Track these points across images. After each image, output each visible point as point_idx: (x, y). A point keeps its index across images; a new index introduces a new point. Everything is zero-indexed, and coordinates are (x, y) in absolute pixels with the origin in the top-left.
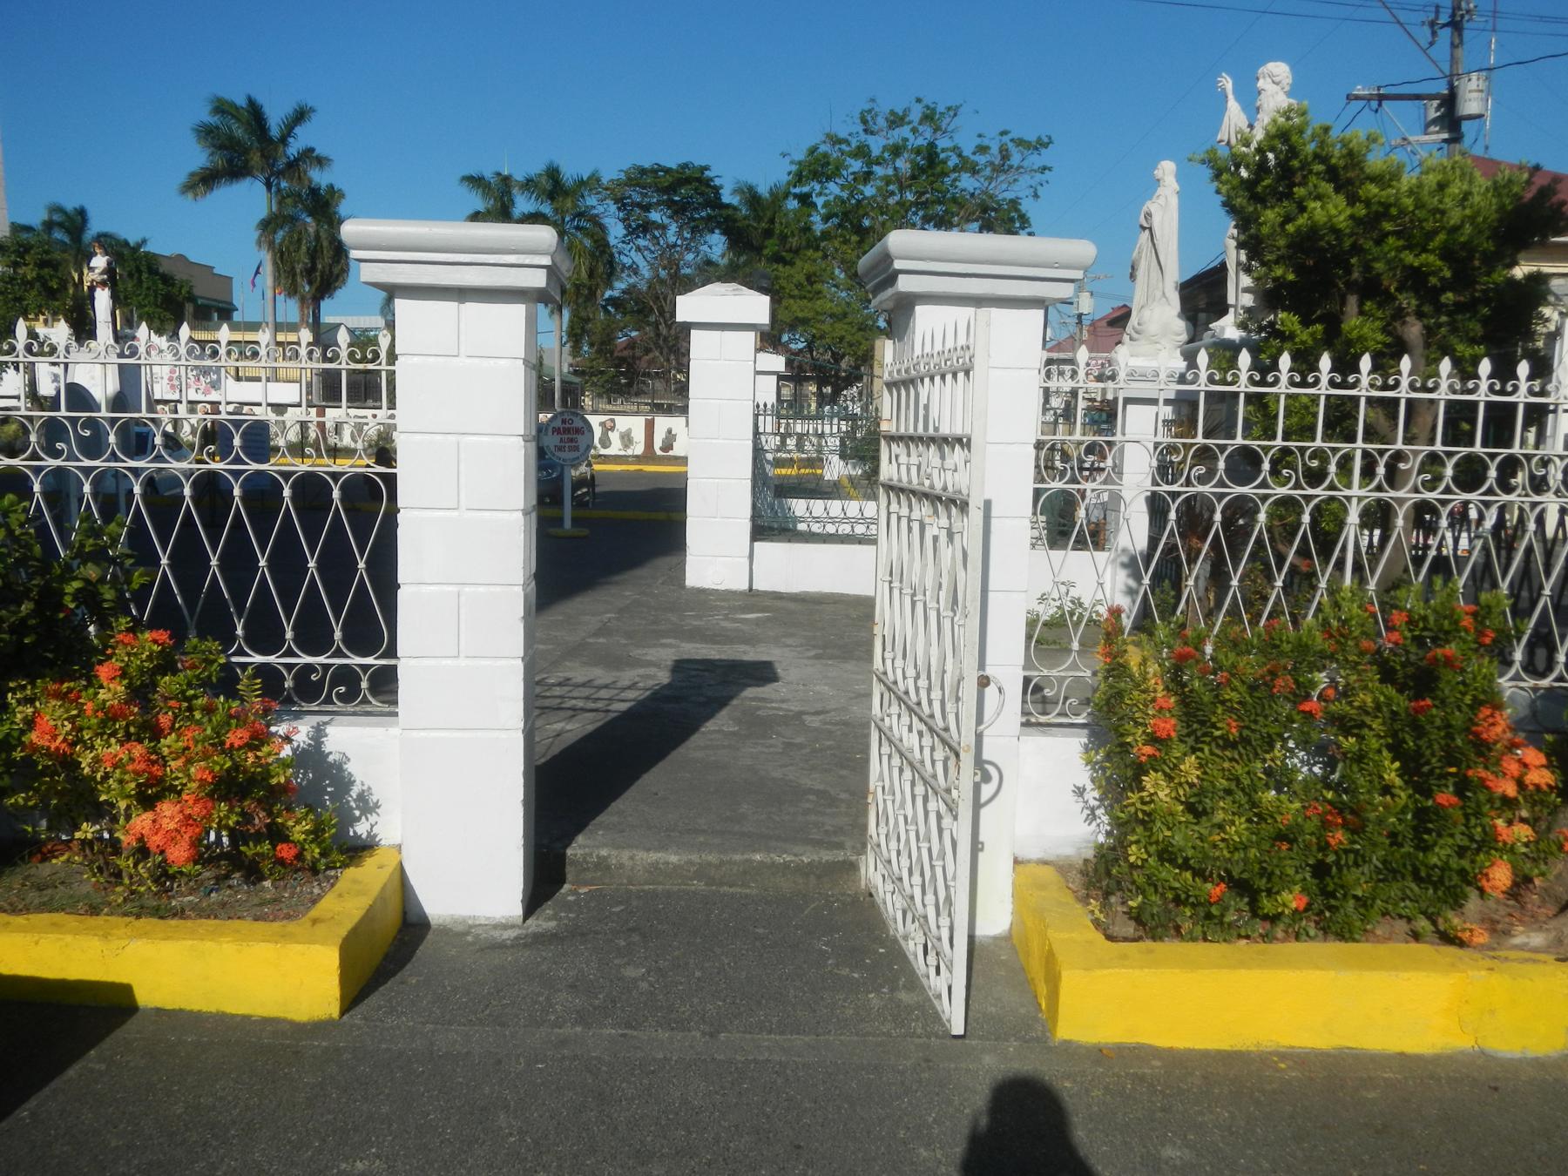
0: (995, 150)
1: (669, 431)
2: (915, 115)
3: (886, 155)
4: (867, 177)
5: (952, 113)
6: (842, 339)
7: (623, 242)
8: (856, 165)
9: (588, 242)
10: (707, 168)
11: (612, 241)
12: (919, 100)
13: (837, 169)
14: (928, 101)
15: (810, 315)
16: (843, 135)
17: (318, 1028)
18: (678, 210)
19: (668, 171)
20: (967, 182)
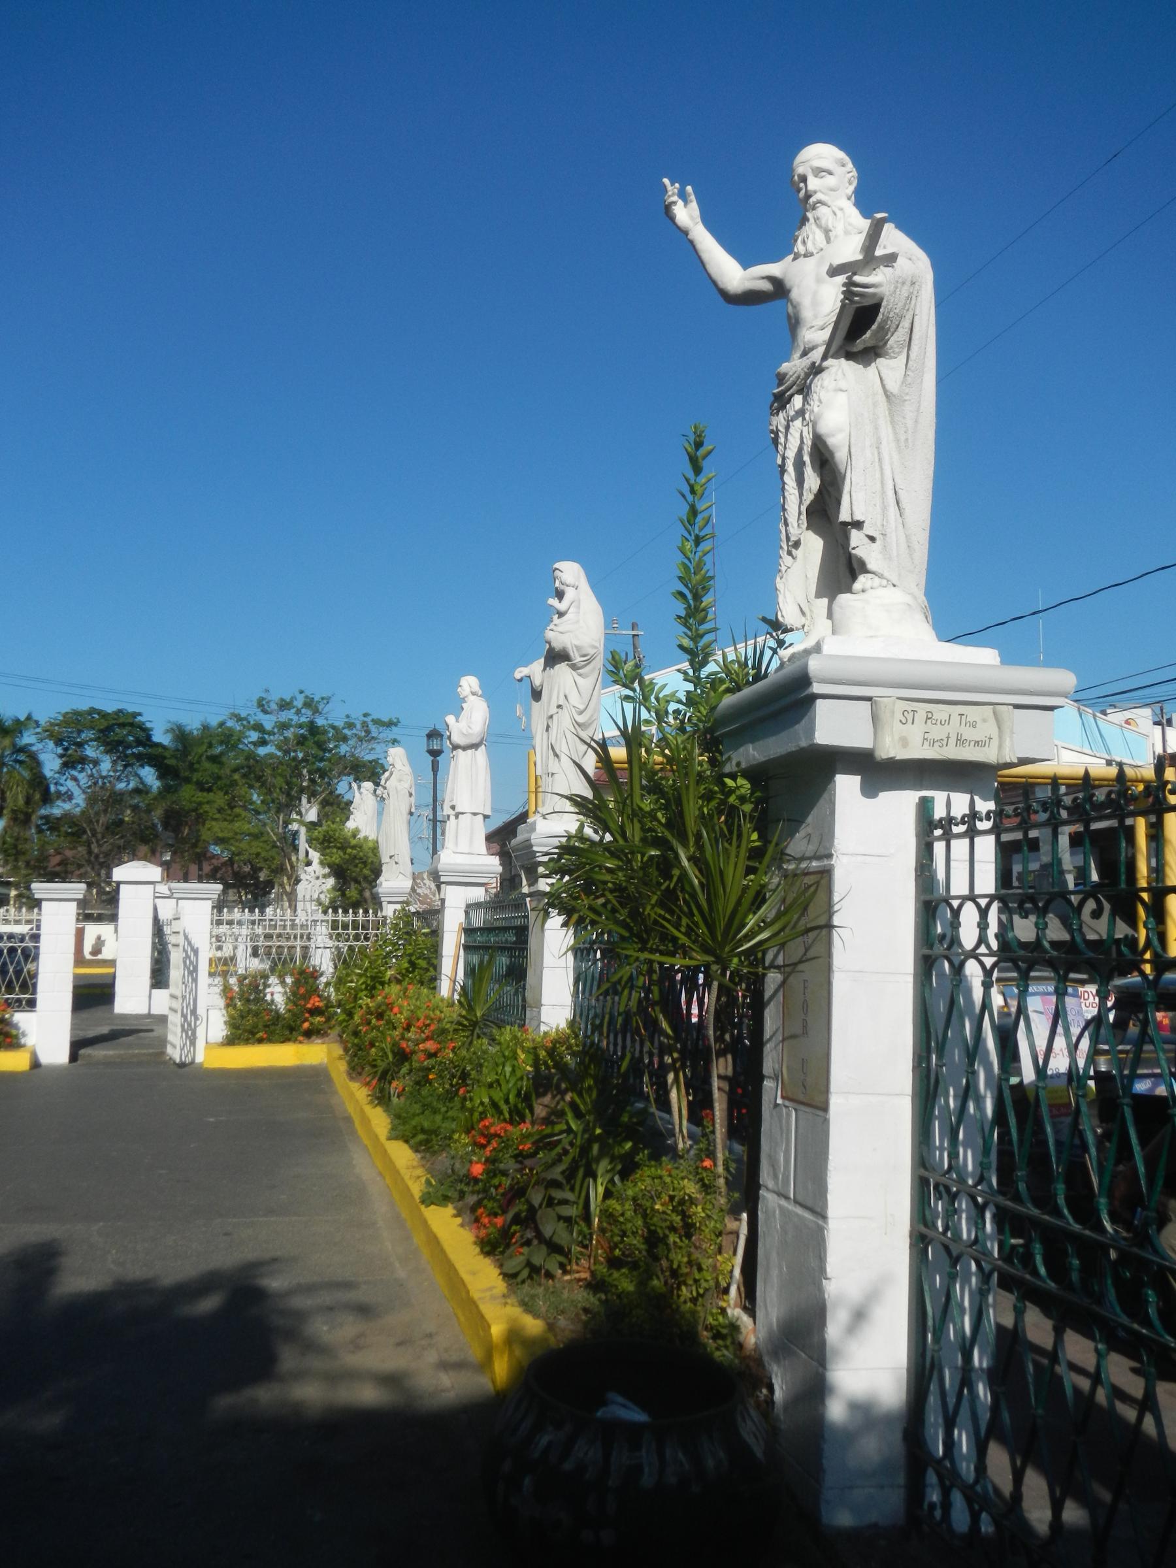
0: (359, 726)
1: (99, 938)
2: (299, 703)
3: (276, 730)
4: (264, 743)
5: (325, 701)
6: (258, 854)
7: (59, 773)
8: (254, 736)
9: (26, 774)
10: (140, 714)
11: (48, 773)
12: (301, 692)
13: (239, 740)
14: (308, 693)
15: (230, 835)
16: (243, 715)
17: (22, 1073)
18: (112, 746)
19: (104, 715)
20: (344, 749)
